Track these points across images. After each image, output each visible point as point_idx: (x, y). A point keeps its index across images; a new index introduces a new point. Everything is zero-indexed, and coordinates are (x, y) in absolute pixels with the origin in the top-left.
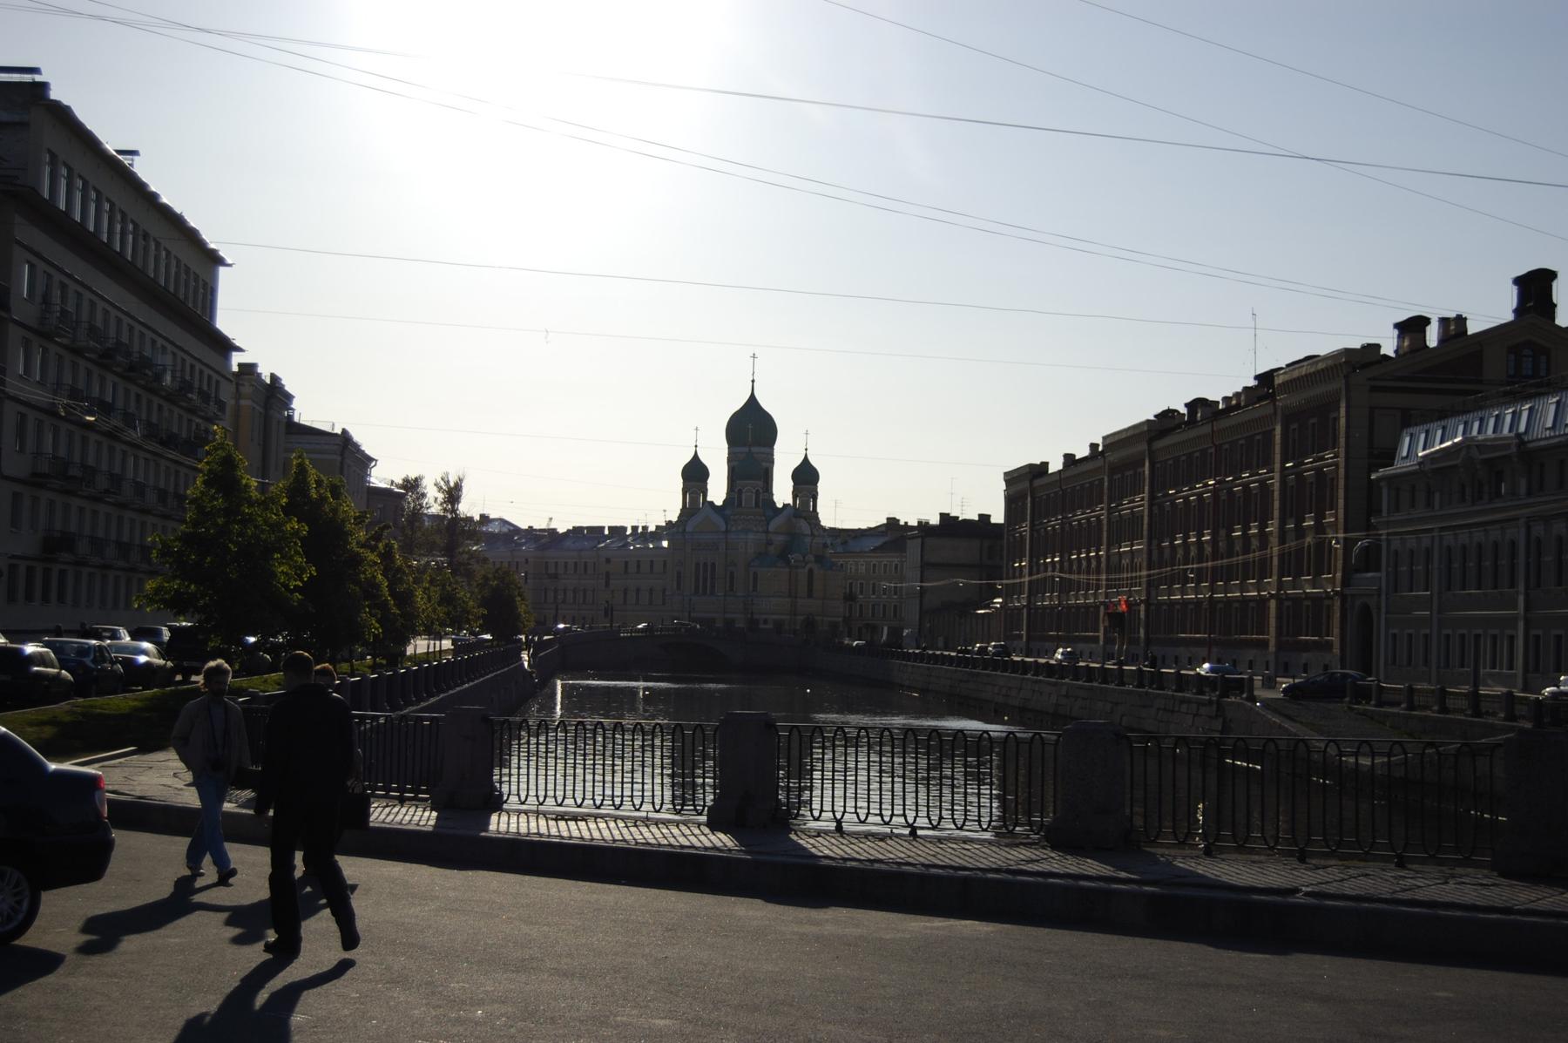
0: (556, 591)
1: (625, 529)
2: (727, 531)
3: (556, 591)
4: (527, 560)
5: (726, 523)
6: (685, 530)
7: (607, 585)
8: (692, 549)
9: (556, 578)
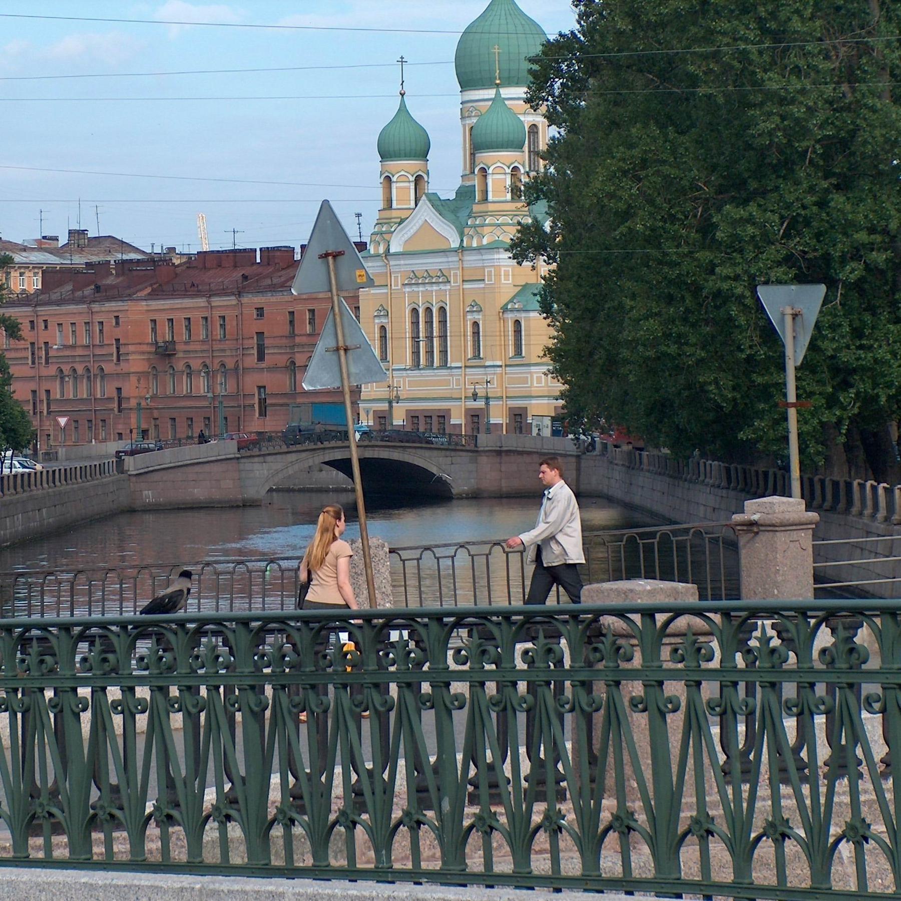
2: (462, 249)
5: (462, 235)
6: (388, 249)
7: (261, 357)
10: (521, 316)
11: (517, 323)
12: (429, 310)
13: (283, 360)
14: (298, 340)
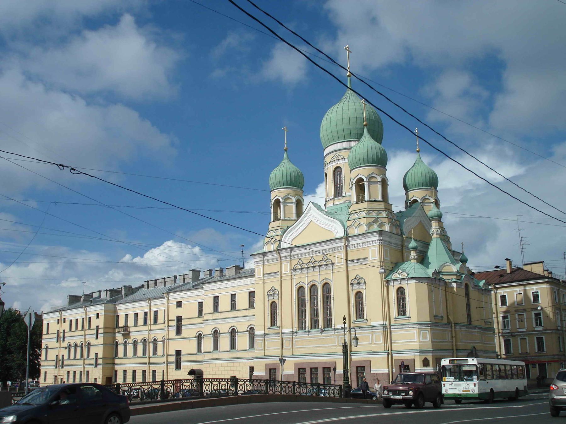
0: (126, 344)
1: (199, 271)
2: (347, 237)
3: (126, 344)
4: (98, 315)
5: (344, 226)
7: (179, 331)
8: (291, 270)
9: (126, 330)
10: (404, 284)
11: (401, 292)
12: (313, 287)
13: (194, 334)
14: (206, 317)
